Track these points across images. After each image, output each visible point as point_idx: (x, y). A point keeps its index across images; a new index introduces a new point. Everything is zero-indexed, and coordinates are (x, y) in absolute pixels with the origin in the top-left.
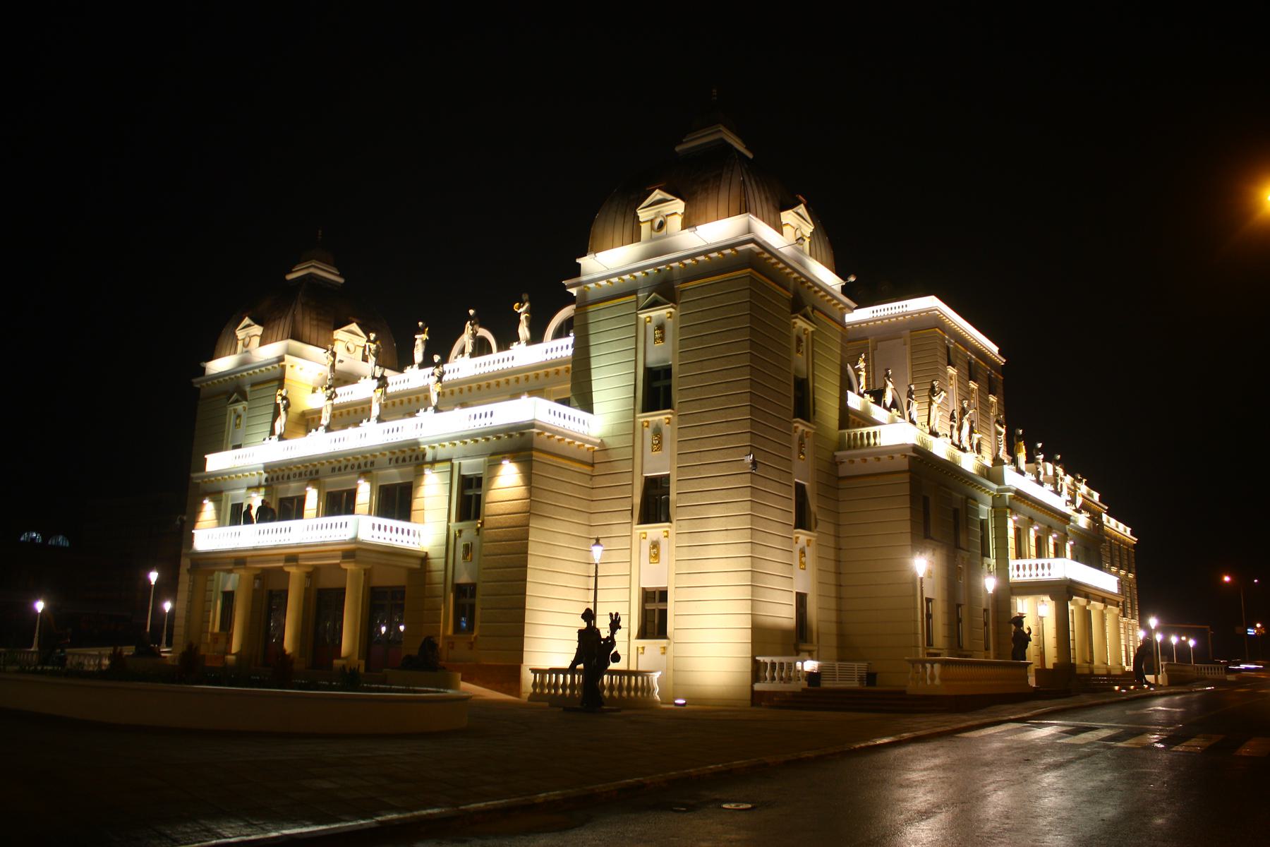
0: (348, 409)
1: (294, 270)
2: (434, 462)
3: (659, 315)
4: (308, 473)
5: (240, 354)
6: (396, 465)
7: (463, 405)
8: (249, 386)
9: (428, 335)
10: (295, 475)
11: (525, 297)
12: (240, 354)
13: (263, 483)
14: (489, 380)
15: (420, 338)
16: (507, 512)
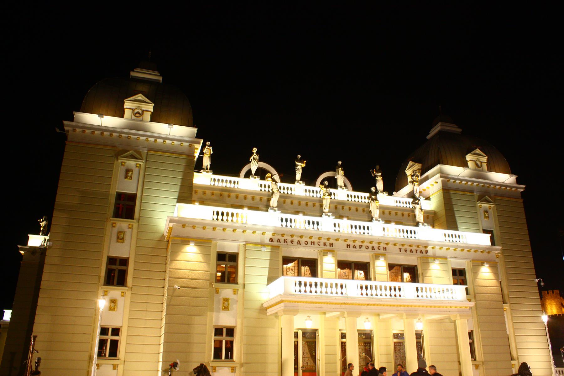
0: (229, 193)
1: (135, 70)
2: (435, 257)
3: (485, 206)
4: (322, 244)
5: (128, 119)
6: (405, 253)
7: (398, 223)
8: (146, 149)
9: (306, 164)
10: (306, 243)
11: (378, 167)
12: (128, 119)
13: (267, 241)
14: (398, 211)
15: (300, 165)
16: (489, 292)
